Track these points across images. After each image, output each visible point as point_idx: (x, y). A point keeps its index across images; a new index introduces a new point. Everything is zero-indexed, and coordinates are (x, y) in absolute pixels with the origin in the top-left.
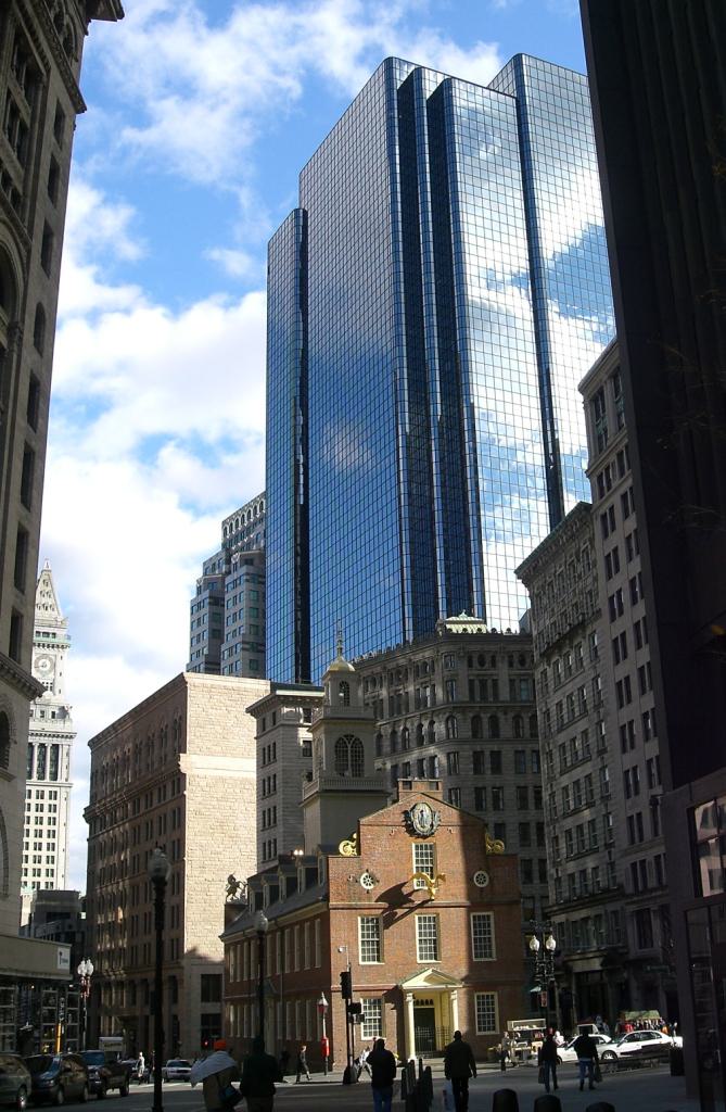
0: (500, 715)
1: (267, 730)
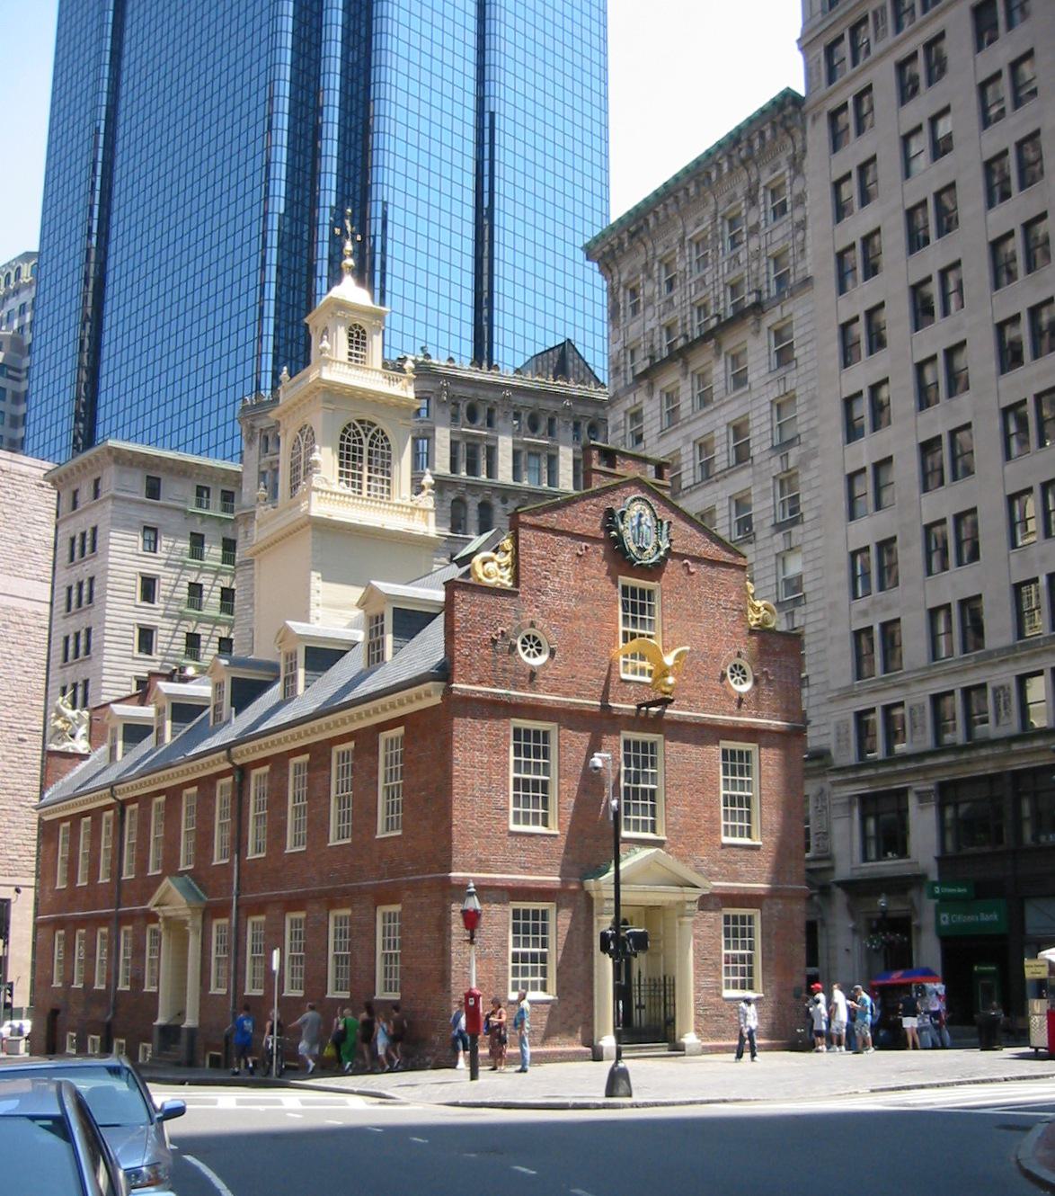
0: (496, 502)
1: (81, 507)
